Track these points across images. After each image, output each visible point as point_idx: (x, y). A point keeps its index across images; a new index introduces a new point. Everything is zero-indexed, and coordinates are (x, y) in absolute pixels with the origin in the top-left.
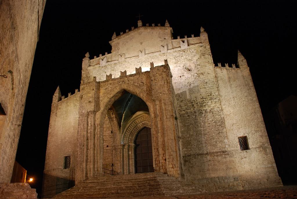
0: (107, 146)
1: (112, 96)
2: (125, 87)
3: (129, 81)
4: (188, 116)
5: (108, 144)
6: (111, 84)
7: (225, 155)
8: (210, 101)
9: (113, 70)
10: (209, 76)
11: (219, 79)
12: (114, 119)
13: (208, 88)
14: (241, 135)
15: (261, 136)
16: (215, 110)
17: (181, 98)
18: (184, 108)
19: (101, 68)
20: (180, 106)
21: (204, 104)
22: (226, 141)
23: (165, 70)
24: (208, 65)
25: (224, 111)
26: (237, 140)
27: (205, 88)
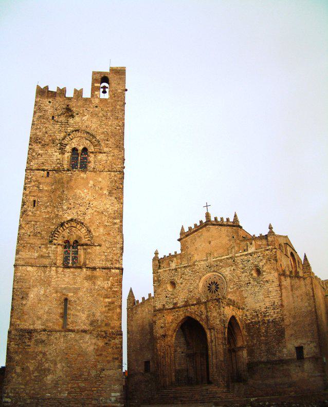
0: (182, 353)
1: (179, 321)
2: (188, 314)
3: (191, 309)
4: (253, 325)
5: (182, 351)
6: (177, 311)
7: (283, 363)
8: (272, 311)
9: (184, 274)
10: (273, 284)
11: (283, 287)
12: (186, 330)
13: (271, 297)
14: (297, 345)
15: (315, 347)
16: (277, 320)
17: (247, 307)
18: (249, 317)
19: (171, 271)
20: (246, 316)
21: (268, 314)
22: (285, 350)
23: (217, 303)
24: (273, 272)
25: (285, 321)
26: (294, 350)
27: (269, 297)
